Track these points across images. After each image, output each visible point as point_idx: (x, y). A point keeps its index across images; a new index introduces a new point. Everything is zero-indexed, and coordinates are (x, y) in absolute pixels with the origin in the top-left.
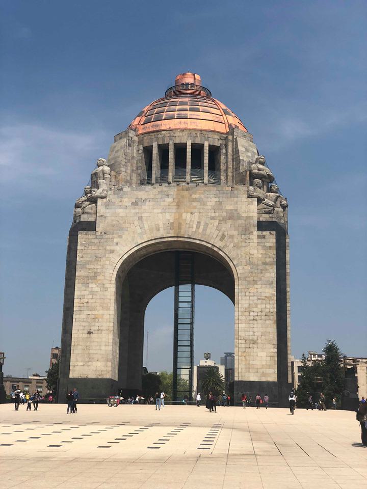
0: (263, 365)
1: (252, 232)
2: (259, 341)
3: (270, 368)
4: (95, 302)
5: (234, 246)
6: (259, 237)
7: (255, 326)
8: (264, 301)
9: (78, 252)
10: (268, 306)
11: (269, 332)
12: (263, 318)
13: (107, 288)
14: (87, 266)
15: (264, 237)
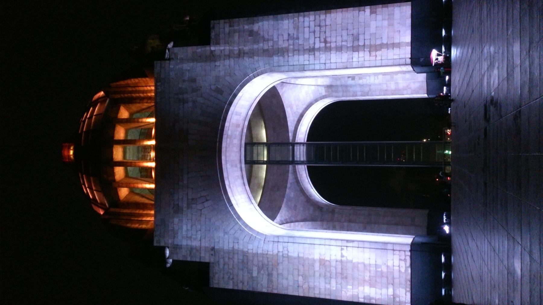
0: (389, 25)
1: (212, 52)
2: (355, 32)
3: (394, 14)
4: (303, 266)
5: (230, 76)
6: (217, 43)
7: (334, 39)
8: (301, 29)
9: (236, 288)
10: (306, 24)
11: (342, 19)
12: (323, 29)
13: (283, 248)
14: (255, 274)
15: (218, 35)
